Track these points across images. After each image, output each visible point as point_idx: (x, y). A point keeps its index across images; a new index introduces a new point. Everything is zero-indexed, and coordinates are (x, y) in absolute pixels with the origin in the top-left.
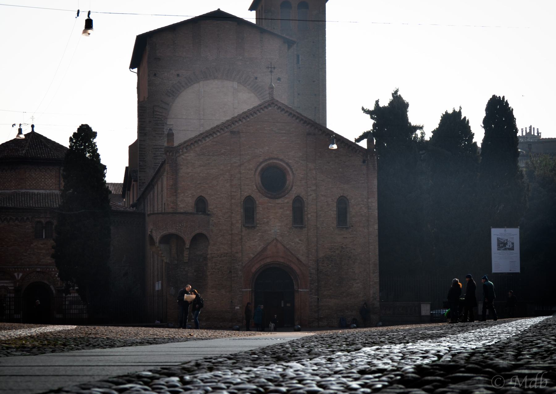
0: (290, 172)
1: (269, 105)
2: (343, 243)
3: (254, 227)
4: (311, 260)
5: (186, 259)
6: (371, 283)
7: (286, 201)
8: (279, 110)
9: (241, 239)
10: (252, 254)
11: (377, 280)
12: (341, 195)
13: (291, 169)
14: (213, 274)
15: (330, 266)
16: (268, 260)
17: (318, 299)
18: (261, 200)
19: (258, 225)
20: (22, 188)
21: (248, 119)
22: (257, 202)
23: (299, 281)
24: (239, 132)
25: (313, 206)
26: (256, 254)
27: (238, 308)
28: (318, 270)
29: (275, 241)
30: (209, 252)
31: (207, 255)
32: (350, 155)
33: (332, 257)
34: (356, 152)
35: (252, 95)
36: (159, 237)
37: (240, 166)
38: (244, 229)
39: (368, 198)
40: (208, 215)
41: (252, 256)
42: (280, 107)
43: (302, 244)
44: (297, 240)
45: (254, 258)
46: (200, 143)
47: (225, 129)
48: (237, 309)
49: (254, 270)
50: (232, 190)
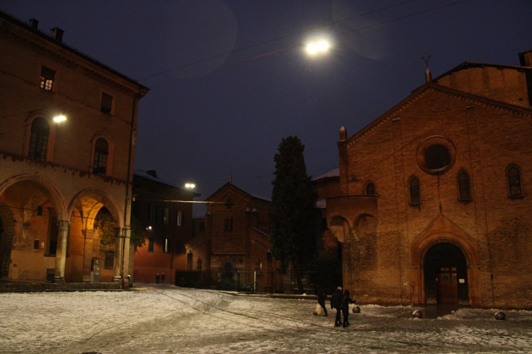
0: (452, 148)
2: (518, 214)
4: (480, 234)
9: (406, 217)
10: (418, 231)
12: (510, 163)
14: (382, 252)
15: (504, 239)
16: (435, 236)
17: (492, 276)
18: (425, 178)
19: (423, 202)
23: (469, 257)
25: (478, 178)
27: (406, 284)
28: (489, 244)
30: (378, 231)
31: (376, 233)
32: (517, 120)
33: (505, 230)
34: (523, 115)
37: (402, 148)
41: (418, 232)
43: (469, 218)
45: (420, 234)
46: (366, 134)
47: (387, 118)
48: (405, 286)
49: (421, 246)
50: (397, 171)
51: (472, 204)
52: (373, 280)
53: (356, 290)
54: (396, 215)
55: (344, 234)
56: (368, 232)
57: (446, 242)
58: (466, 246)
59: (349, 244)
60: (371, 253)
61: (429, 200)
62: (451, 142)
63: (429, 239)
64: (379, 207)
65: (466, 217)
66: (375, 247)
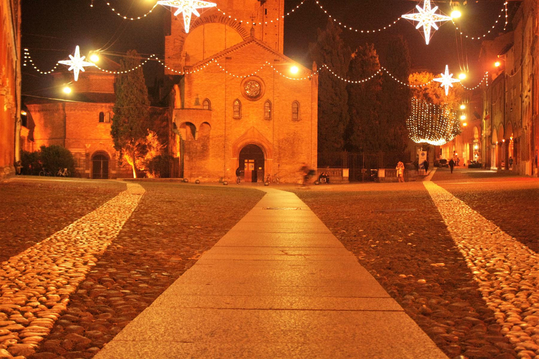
1: (251, 41)
3: (239, 119)
5: (196, 139)
6: (312, 156)
7: (260, 103)
8: (257, 45)
9: (231, 126)
11: (316, 154)
13: (264, 83)
15: (287, 145)
16: (248, 140)
20: (90, 90)
21: (237, 50)
22: (242, 103)
24: (231, 58)
26: (240, 136)
27: (228, 170)
29: (252, 128)
30: (211, 134)
35: (237, 33)
36: (179, 124)
38: (233, 120)
39: (312, 102)
40: (211, 110)
41: (238, 137)
42: (258, 43)
44: (267, 128)
45: (239, 139)
47: (222, 56)
49: (239, 146)
51: (272, 121)
52: (206, 167)
53: (194, 173)
54: (224, 124)
55: (186, 135)
56: (204, 134)
57: (254, 144)
58: (266, 147)
59: (190, 142)
60: (205, 149)
61: (246, 116)
62: (263, 81)
63: (244, 142)
64: (212, 118)
65: (267, 130)
66: (208, 145)
